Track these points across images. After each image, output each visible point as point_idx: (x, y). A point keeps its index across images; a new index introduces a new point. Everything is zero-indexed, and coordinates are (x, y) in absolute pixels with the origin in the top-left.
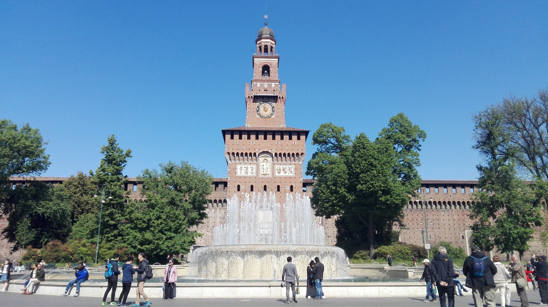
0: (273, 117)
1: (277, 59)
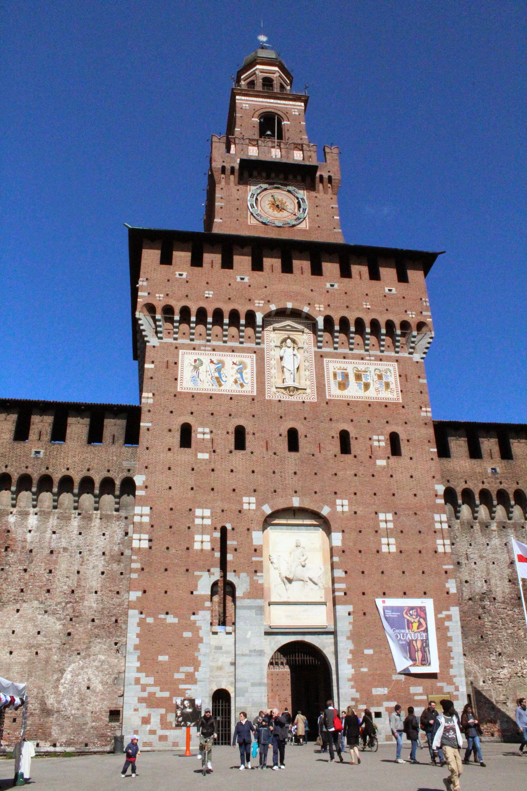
0: (303, 226)
1: (303, 104)
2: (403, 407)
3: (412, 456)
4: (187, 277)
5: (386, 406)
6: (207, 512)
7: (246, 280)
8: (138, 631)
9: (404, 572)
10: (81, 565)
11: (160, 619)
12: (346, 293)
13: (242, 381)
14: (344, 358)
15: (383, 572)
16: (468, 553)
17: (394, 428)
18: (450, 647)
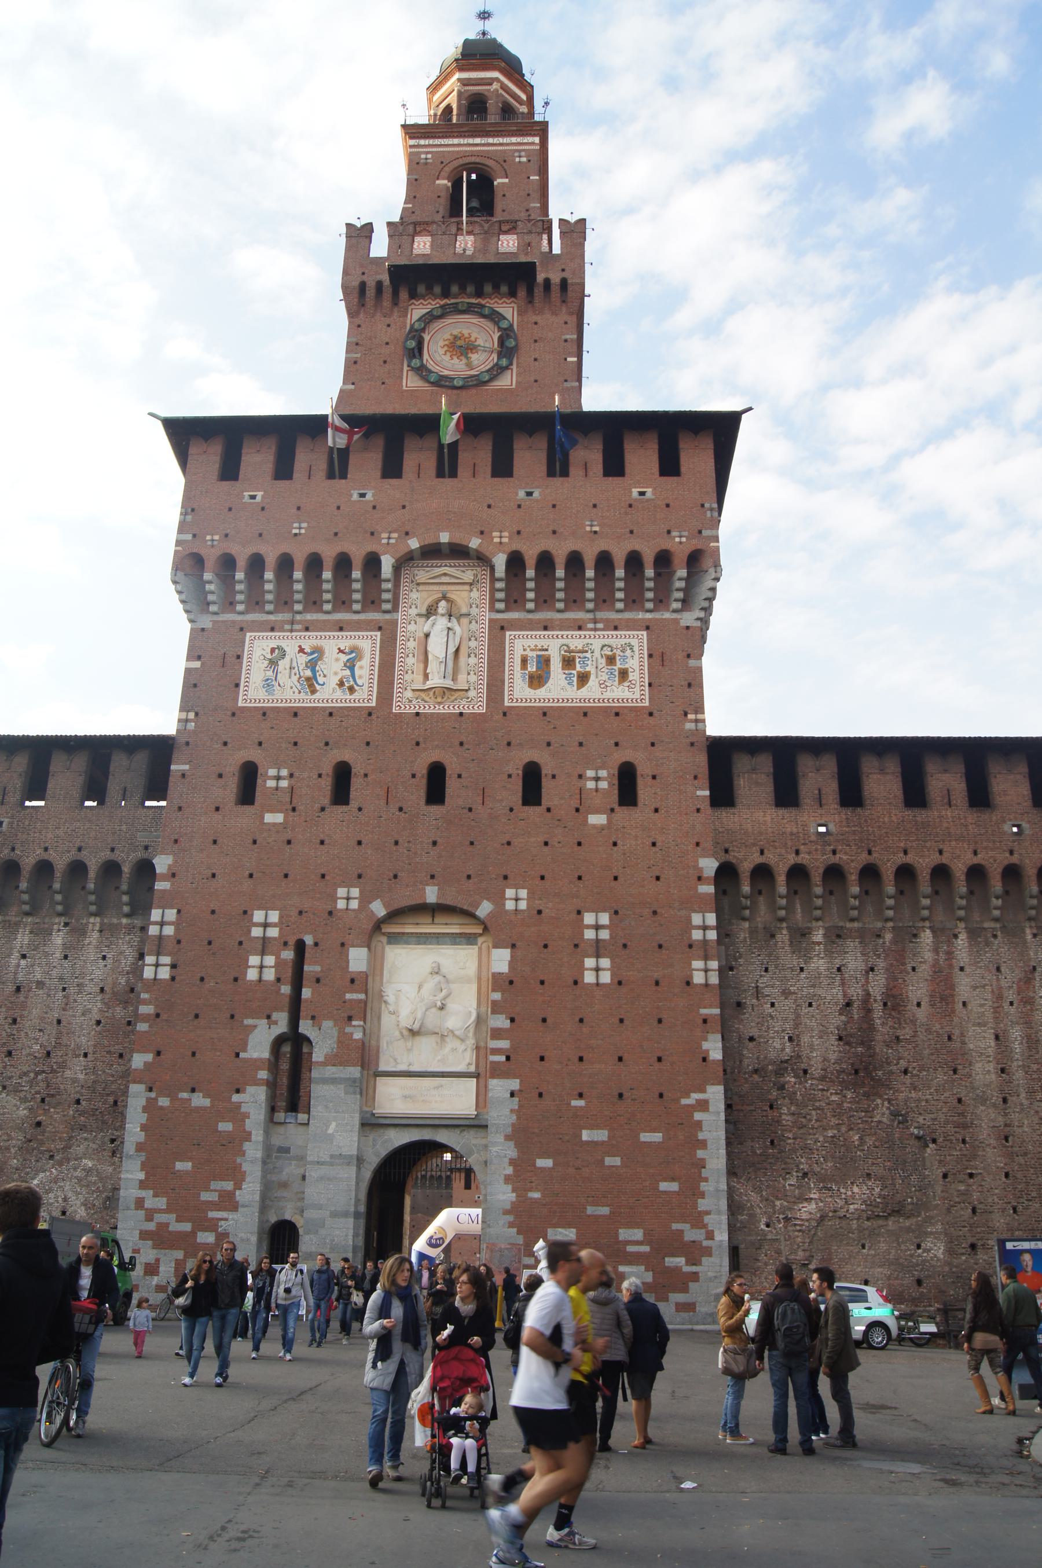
0: (507, 381)
1: (537, 140)
2: (651, 714)
3: (658, 805)
4: (262, 501)
5: (617, 714)
6: (274, 916)
8: (144, 1121)
9: (621, 1021)
10: (64, 1010)
11: (182, 1099)
12: (554, 506)
13: (352, 683)
14: (546, 628)
15: (581, 1020)
16: (761, 985)
18: (703, 1160)
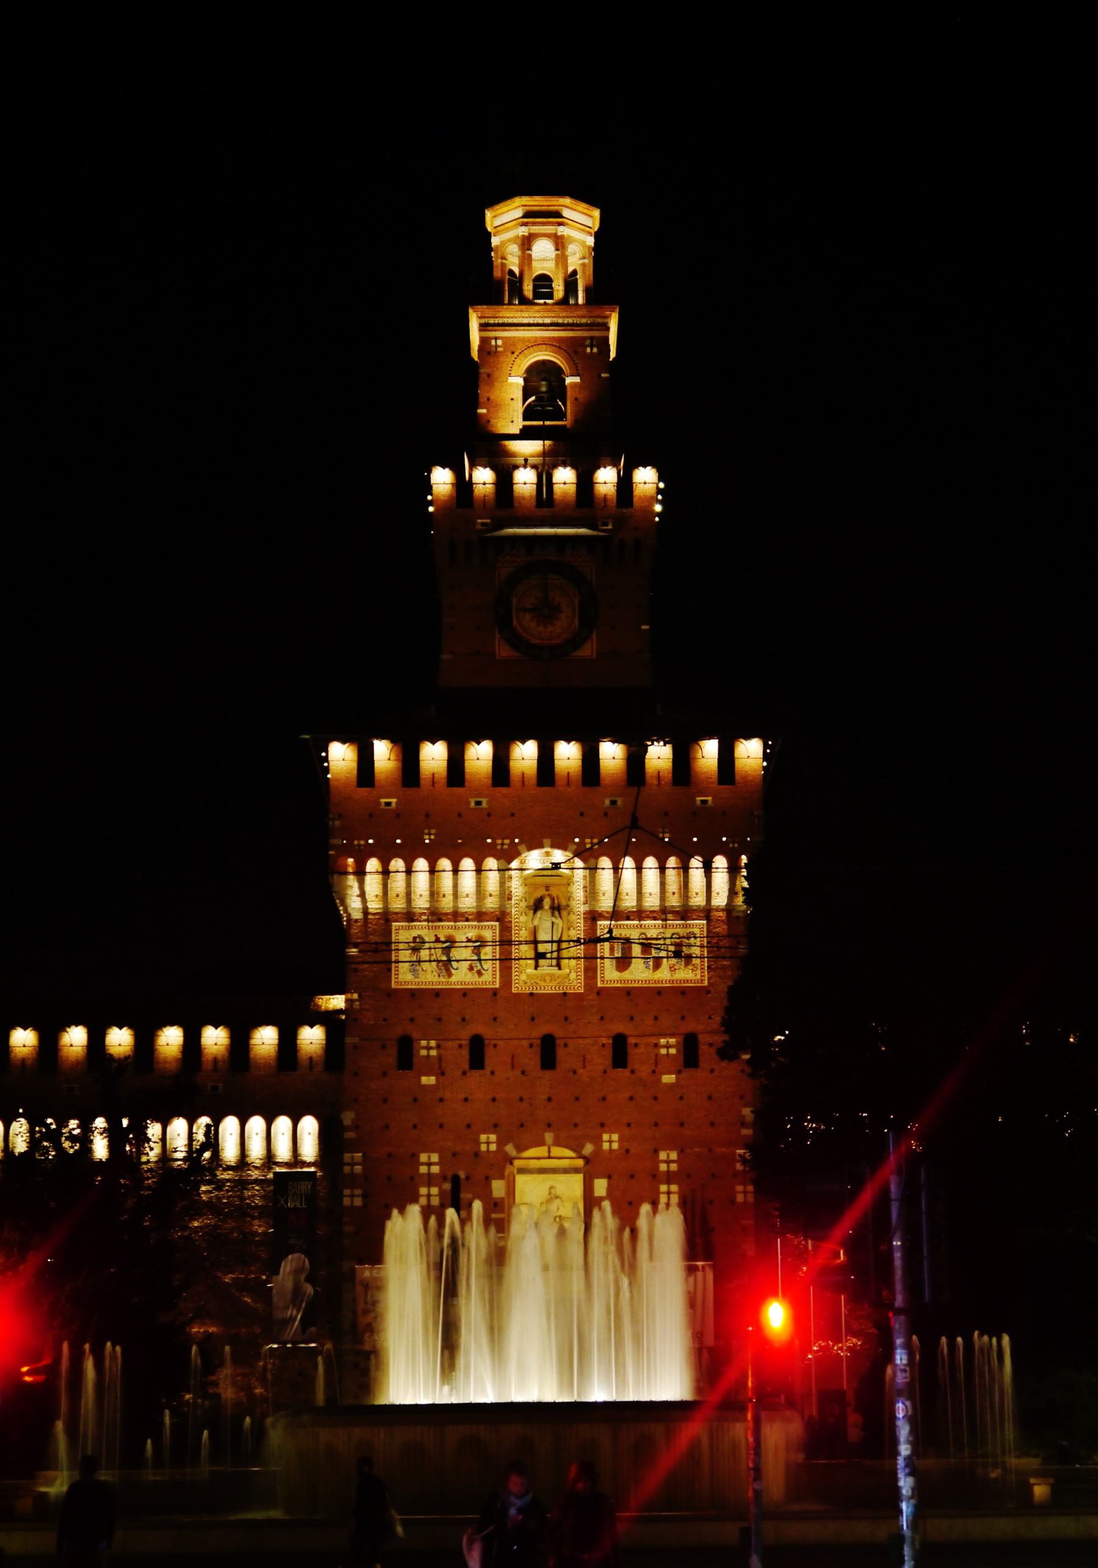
0: (587, 651)
6: (435, 1158)
7: (484, 805)
13: (479, 967)
17: (691, 1026)
